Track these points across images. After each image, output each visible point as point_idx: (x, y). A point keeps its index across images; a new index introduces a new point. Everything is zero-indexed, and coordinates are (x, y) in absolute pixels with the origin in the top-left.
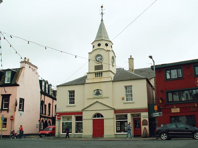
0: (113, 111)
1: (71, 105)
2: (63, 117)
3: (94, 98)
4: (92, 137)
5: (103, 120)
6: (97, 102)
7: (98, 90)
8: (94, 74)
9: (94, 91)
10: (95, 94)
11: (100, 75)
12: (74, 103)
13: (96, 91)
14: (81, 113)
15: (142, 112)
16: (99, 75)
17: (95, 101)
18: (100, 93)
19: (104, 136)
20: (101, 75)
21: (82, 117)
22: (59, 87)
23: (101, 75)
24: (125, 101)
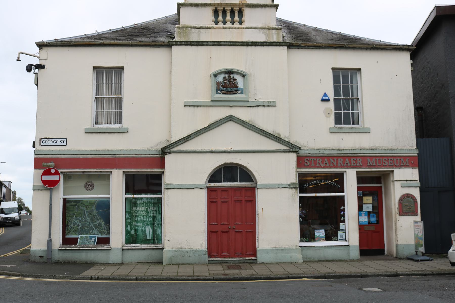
0: (293, 157)
2: (68, 177)
3: (214, 104)
6: (231, 118)
7: (230, 72)
8: (208, 13)
9: (215, 76)
13: (220, 78)
14: (161, 163)
15: (400, 167)
16: (228, 18)
17: (223, 113)
18: (241, 85)
19: (261, 257)
20: (236, 18)
21: (159, 177)
22: (45, 49)
23: (236, 18)
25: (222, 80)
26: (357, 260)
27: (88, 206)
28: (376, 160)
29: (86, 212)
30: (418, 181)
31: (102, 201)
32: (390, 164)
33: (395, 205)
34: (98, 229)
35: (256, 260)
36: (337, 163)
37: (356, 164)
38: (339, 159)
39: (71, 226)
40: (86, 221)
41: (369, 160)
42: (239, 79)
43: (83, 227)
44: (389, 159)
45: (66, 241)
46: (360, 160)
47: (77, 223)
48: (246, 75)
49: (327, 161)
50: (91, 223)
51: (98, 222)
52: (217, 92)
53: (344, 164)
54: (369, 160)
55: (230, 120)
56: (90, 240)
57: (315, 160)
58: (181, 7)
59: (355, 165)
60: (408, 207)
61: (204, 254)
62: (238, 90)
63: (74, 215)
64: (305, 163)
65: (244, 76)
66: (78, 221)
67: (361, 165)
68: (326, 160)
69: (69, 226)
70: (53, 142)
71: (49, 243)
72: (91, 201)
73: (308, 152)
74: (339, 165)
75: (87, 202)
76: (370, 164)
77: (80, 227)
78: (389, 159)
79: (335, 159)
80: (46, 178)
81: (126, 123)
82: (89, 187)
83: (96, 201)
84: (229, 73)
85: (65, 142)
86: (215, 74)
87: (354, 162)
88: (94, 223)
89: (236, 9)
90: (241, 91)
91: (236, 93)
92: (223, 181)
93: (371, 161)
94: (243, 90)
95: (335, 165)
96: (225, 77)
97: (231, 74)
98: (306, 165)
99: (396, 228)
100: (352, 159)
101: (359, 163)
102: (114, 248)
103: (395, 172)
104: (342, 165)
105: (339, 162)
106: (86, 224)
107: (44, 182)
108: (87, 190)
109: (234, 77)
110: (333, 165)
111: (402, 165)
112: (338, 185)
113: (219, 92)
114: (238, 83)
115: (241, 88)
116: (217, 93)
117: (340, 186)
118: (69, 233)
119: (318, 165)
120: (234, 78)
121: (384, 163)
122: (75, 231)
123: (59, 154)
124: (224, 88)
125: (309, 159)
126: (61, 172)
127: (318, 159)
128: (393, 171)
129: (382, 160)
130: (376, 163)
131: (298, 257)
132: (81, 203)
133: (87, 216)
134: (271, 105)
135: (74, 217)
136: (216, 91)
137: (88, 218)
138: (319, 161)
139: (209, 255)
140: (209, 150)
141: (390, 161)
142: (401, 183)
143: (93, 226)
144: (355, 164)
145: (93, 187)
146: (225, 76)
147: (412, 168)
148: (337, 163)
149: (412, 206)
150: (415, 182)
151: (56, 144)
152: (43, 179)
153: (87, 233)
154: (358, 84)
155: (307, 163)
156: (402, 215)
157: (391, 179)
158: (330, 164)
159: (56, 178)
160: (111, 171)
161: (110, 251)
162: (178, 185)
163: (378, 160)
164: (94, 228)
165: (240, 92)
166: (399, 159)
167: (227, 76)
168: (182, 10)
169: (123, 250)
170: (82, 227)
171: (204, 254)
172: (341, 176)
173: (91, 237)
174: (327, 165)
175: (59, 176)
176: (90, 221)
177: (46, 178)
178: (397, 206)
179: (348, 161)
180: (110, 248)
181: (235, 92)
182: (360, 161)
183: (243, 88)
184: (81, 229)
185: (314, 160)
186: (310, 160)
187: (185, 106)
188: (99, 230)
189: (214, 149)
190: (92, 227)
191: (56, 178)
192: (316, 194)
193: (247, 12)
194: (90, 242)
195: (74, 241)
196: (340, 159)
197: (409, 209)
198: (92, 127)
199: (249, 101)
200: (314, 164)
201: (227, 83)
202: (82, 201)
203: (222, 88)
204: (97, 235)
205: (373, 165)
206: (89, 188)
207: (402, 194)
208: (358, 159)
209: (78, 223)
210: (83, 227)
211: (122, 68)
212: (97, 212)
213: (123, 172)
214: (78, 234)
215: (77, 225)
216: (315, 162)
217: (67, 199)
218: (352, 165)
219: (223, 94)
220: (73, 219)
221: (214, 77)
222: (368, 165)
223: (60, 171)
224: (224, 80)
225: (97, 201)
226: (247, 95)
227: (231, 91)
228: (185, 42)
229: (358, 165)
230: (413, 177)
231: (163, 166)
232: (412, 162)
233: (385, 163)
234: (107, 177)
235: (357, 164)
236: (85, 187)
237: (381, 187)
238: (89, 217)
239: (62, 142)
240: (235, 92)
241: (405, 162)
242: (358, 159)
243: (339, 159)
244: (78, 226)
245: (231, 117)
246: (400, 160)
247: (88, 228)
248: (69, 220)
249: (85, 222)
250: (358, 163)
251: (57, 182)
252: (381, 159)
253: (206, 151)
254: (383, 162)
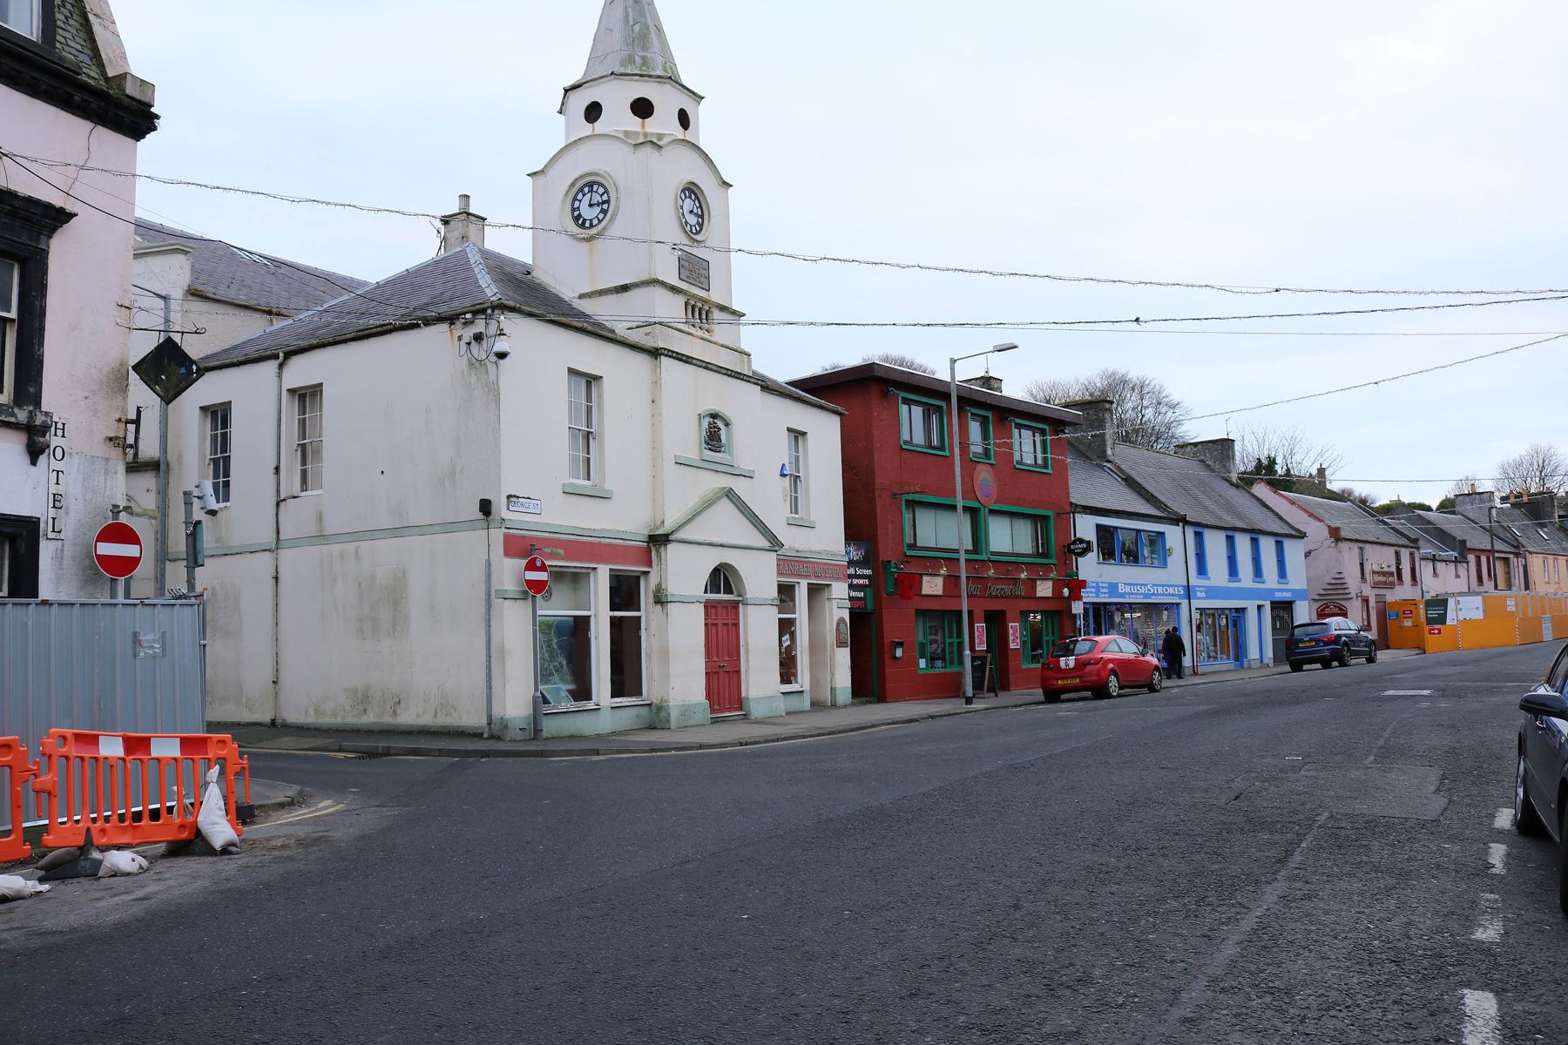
5: (735, 605)
7: (714, 416)
26: (807, 712)
31: (561, 622)
65: (727, 425)
72: (548, 622)
103: (833, 586)
107: (529, 583)
131: (781, 706)
167: (711, 420)
219: (710, 449)
223: (547, 563)
226: (730, 454)
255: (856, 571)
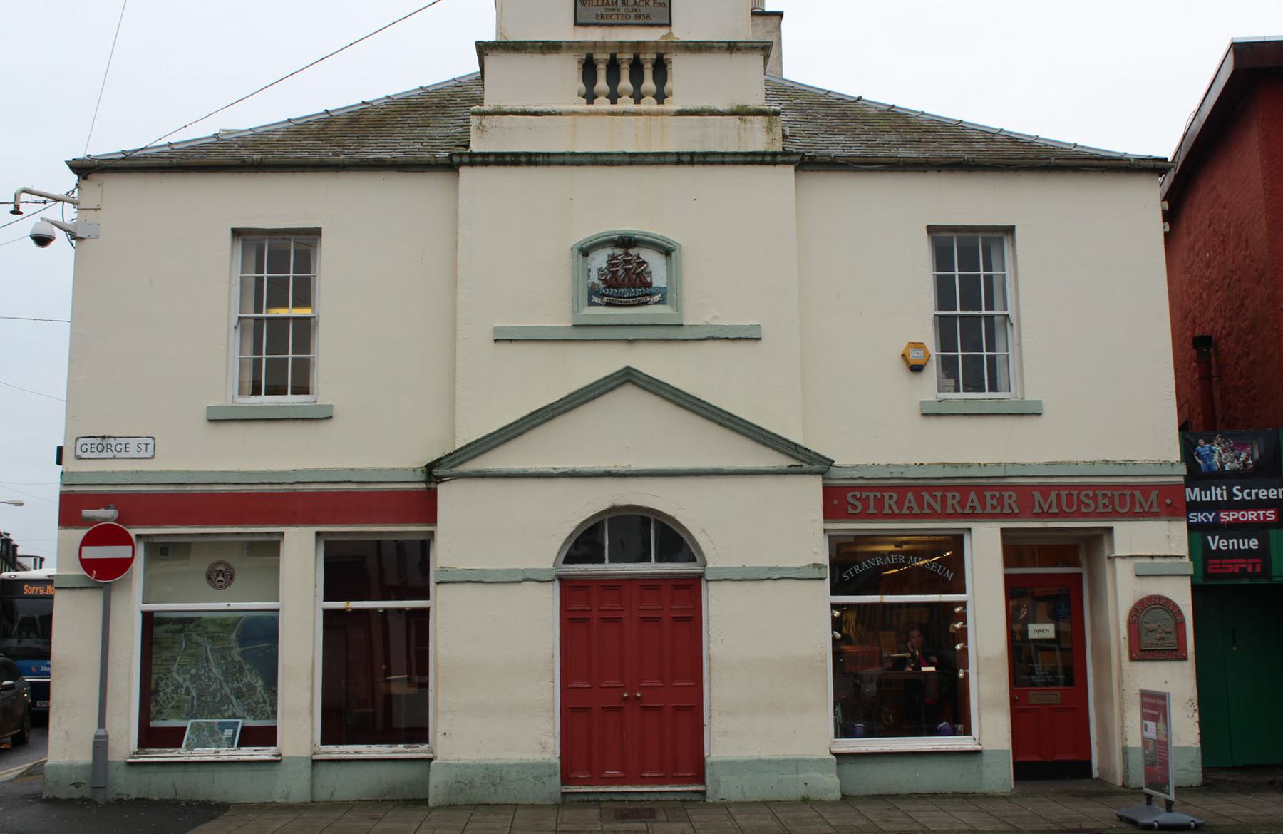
0: (812, 489)
1: (264, 400)
2: (160, 550)
3: (583, 334)
4: (554, 785)
5: (691, 587)
6: (628, 377)
7: (626, 242)
8: (567, 70)
9: (585, 251)
10: (593, 291)
11: (637, 78)
12: (302, 388)
13: (600, 259)
15: (1133, 515)
16: (625, 84)
17: (607, 361)
18: (659, 279)
20: (649, 84)
22: (96, 178)
23: (649, 84)
24: (928, 385)
25: (605, 265)
26: (1004, 797)
27: (216, 634)
28: (1058, 496)
29: (211, 650)
30: (1187, 560)
31: (257, 619)
32: (1101, 509)
33: (1118, 629)
34: (246, 703)
35: (703, 793)
36: (944, 506)
37: (999, 507)
38: (949, 495)
39: (165, 694)
40: (210, 679)
41: (1037, 495)
42: (654, 261)
43: (202, 696)
44: (1099, 493)
45: (150, 737)
46: (1010, 496)
47: (185, 686)
48: (673, 250)
49: (913, 500)
50: (224, 684)
51: (245, 680)
52: (590, 299)
53: (963, 507)
54: (1037, 495)
55: (628, 381)
56: (220, 735)
57: (879, 496)
58: (487, 55)
59: (998, 510)
60: (1158, 636)
61: (548, 774)
62: (651, 295)
63: (175, 660)
64: (850, 507)
66: (187, 677)
67: (1016, 511)
68: (910, 495)
69: (161, 694)
70: (113, 448)
71: (101, 745)
72: (224, 619)
73: (857, 474)
74: (950, 510)
75: (213, 621)
76: (1041, 507)
77: (193, 697)
78: (1099, 493)
79: (939, 494)
80: (95, 552)
81: (325, 388)
82: (220, 578)
83: (241, 617)
84: (623, 243)
85: (150, 448)
86: (584, 246)
87: (992, 502)
88: (233, 683)
89: (649, 57)
90: (660, 295)
91: (646, 303)
92: (607, 560)
93: (1046, 499)
94: (666, 293)
95: (939, 510)
96: (613, 257)
97: (631, 247)
98: (851, 511)
99: (1121, 697)
100: (988, 494)
101: (1010, 507)
102: (289, 757)
104: (959, 510)
105: (950, 501)
106: (211, 686)
107: (87, 564)
108: (214, 586)
109: (641, 256)
110: (930, 512)
111: (1138, 509)
112: (946, 571)
113: (596, 299)
114: (651, 272)
115: (660, 288)
116: (591, 303)
117: (952, 574)
118: (159, 712)
119: (887, 511)
120: (638, 257)
121: (1082, 506)
122: (178, 710)
123: (132, 484)
124: (609, 287)
125: (861, 494)
126: (138, 536)
127: (886, 495)
128: (1110, 530)
129: (1078, 495)
130: (1059, 506)
131: (829, 784)
132: (198, 626)
133: (212, 665)
134: (750, 337)
135: (176, 666)
136: (586, 297)
137: (214, 670)
138: (890, 501)
139: (566, 780)
140: (565, 468)
141: (1101, 501)
142: (1136, 566)
143: (231, 693)
144: (996, 507)
145: (232, 577)
146: (614, 254)
147: (1169, 520)
148: (944, 506)
149: (1170, 632)
150: (1179, 560)
151: (123, 454)
152: (83, 557)
153: (212, 714)
154: (1007, 272)
155: (855, 507)
156: (1137, 660)
157: (1107, 553)
158: (921, 506)
159: (121, 552)
160: (283, 533)
161: (277, 767)
162: (472, 571)
163: (1067, 495)
164: (233, 698)
165: (657, 298)
166: (1128, 493)
167: (619, 252)
168: (490, 60)
169: (315, 762)
170: (198, 695)
171: (550, 776)
172: (956, 542)
173: (223, 727)
174: (913, 512)
175: (130, 548)
176: (222, 679)
177: (95, 552)
178: (1124, 632)
179: (976, 500)
180: (279, 758)
181: (643, 299)
182: (1011, 499)
183: (665, 288)
184: (195, 702)
185: (875, 496)
186: (864, 497)
187: (496, 341)
188: (248, 704)
189: (579, 466)
190: (226, 694)
191: (121, 552)
192: (882, 598)
193: (680, 66)
194: (220, 739)
195: (173, 738)
196: (954, 493)
197: (1160, 643)
198: (229, 403)
199: (682, 325)
200: (876, 508)
201: (619, 274)
202: (200, 618)
203: (604, 288)
204: (241, 721)
205: (1051, 511)
206: (220, 581)
207: (1139, 597)
208: (1006, 494)
209: (187, 683)
210: (200, 696)
211: (318, 232)
212: (243, 652)
213: (318, 534)
214: (187, 715)
215: (184, 689)
216: (879, 503)
217: (156, 615)
218: (989, 510)
219: (608, 304)
220: (173, 671)
221: (580, 256)
222: (1037, 510)
223: (133, 532)
224: (611, 265)
225: (242, 620)
226: (678, 307)
227: (629, 297)
228: (496, 154)
229: (1006, 510)
230: (1172, 544)
231: (430, 515)
232: (1168, 501)
233: (1087, 506)
234: (272, 547)
235: (1003, 508)
236: (209, 577)
237: (1079, 576)
238: (218, 665)
239: (143, 447)
240: (643, 299)
241: (1146, 502)
242: (1006, 494)
243: (949, 495)
244: (188, 692)
245: (628, 374)
246: (1133, 496)
247: (217, 700)
248: (161, 675)
249: (207, 681)
250: (1006, 505)
251: (123, 565)
252: (1075, 493)
253: (555, 472)
254: (1080, 501)
255: (1231, 494)
